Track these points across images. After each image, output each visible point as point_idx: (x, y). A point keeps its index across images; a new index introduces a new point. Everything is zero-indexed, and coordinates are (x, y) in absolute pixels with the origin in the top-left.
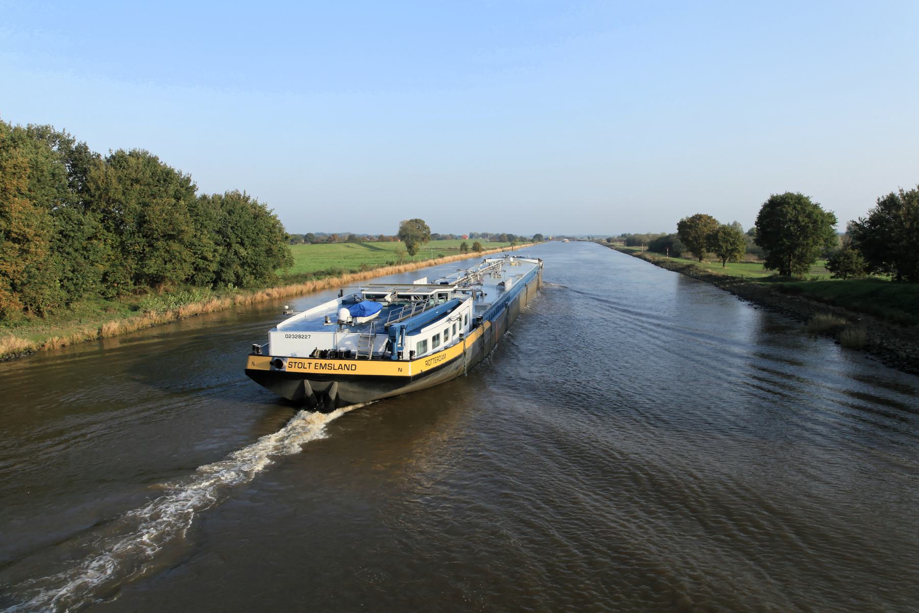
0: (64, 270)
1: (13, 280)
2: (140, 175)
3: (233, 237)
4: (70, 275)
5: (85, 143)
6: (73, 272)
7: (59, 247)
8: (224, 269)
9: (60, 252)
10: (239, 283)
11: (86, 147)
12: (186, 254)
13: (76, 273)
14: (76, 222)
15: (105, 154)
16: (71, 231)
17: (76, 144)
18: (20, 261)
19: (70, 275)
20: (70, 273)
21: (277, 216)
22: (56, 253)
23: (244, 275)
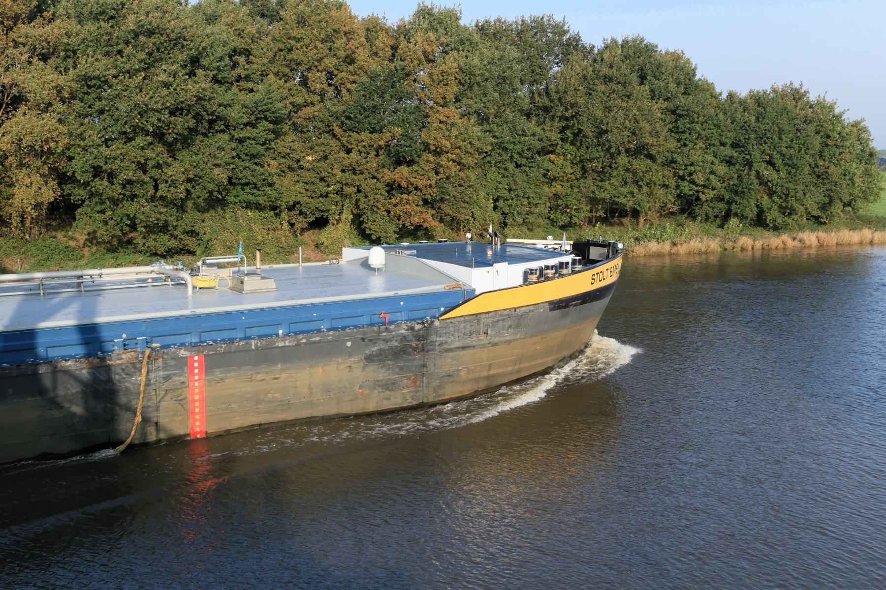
0: (497, 188)
1: (425, 194)
2: (614, 72)
3: (756, 155)
4: (507, 194)
5: (578, 33)
6: (510, 190)
7: (496, 162)
8: (737, 198)
9: (498, 167)
10: (760, 221)
11: (580, 37)
12: (660, 174)
13: (512, 192)
14: (520, 133)
15: (599, 45)
16: (511, 143)
17: (568, 35)
18: (432, 174)
19: (507, 194)
20: (505, 192)
21: (863, 120)
22: (494, 169)
23: (770, 209)
